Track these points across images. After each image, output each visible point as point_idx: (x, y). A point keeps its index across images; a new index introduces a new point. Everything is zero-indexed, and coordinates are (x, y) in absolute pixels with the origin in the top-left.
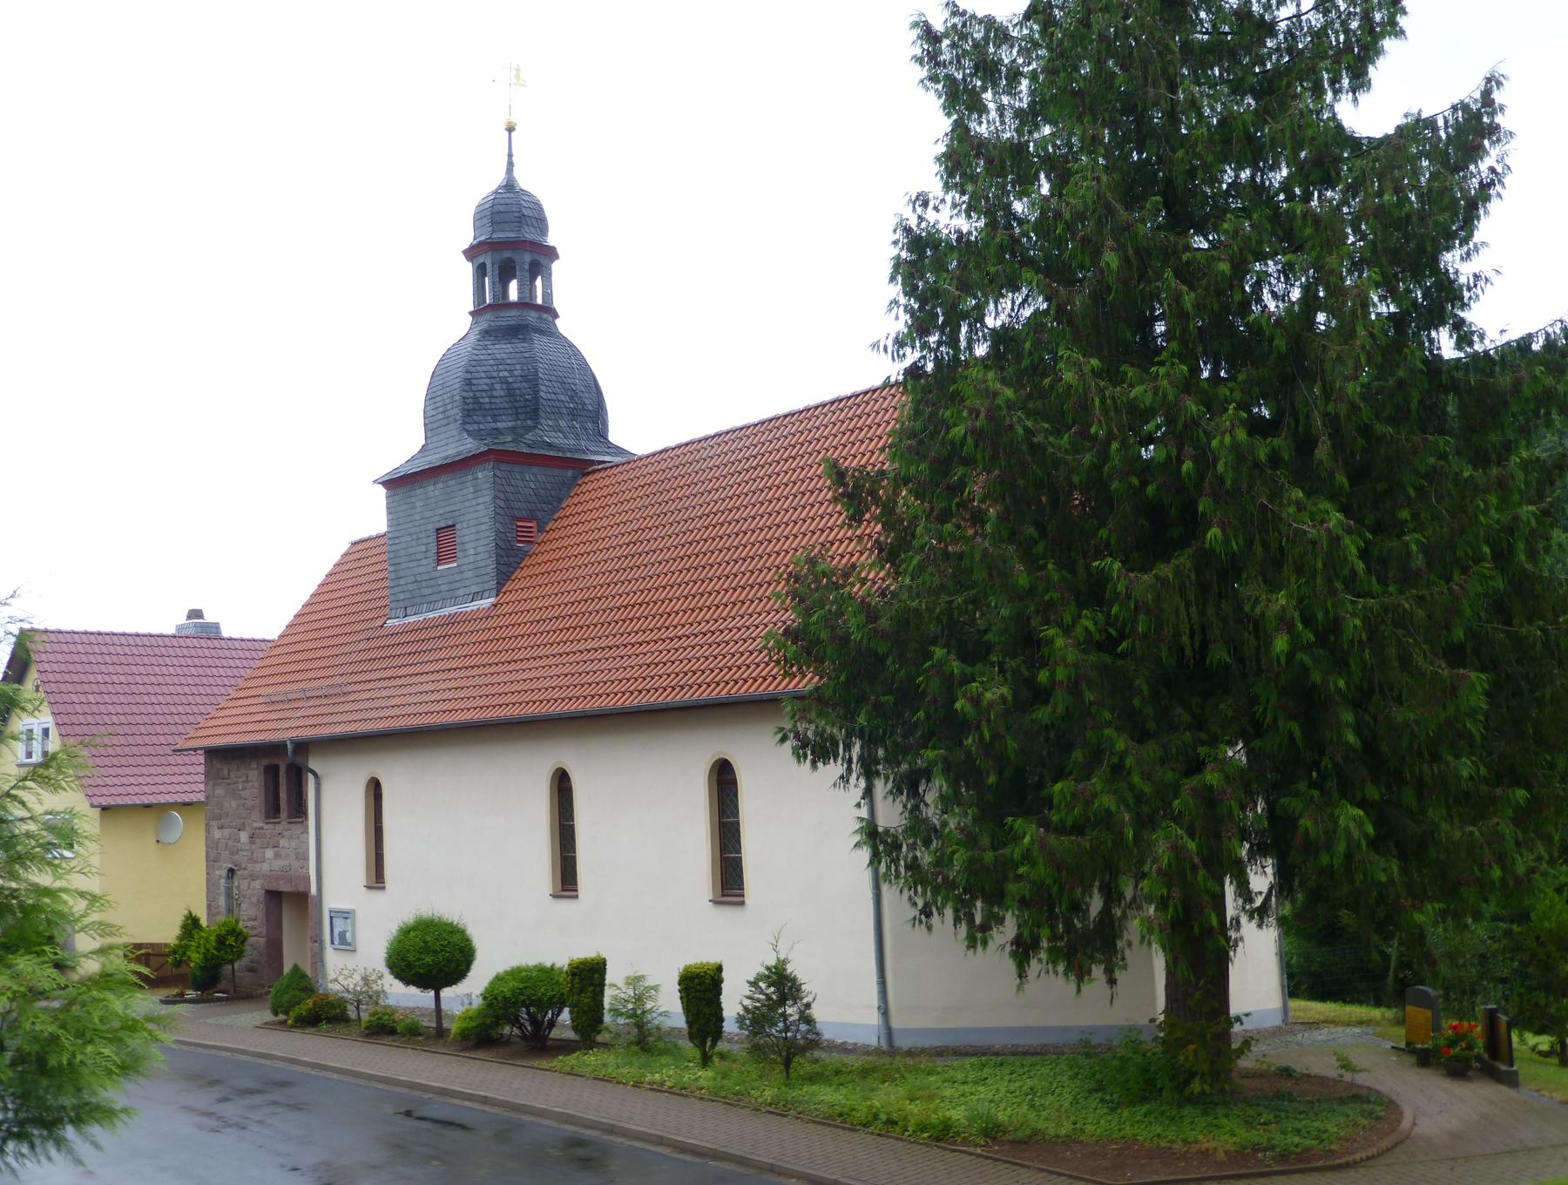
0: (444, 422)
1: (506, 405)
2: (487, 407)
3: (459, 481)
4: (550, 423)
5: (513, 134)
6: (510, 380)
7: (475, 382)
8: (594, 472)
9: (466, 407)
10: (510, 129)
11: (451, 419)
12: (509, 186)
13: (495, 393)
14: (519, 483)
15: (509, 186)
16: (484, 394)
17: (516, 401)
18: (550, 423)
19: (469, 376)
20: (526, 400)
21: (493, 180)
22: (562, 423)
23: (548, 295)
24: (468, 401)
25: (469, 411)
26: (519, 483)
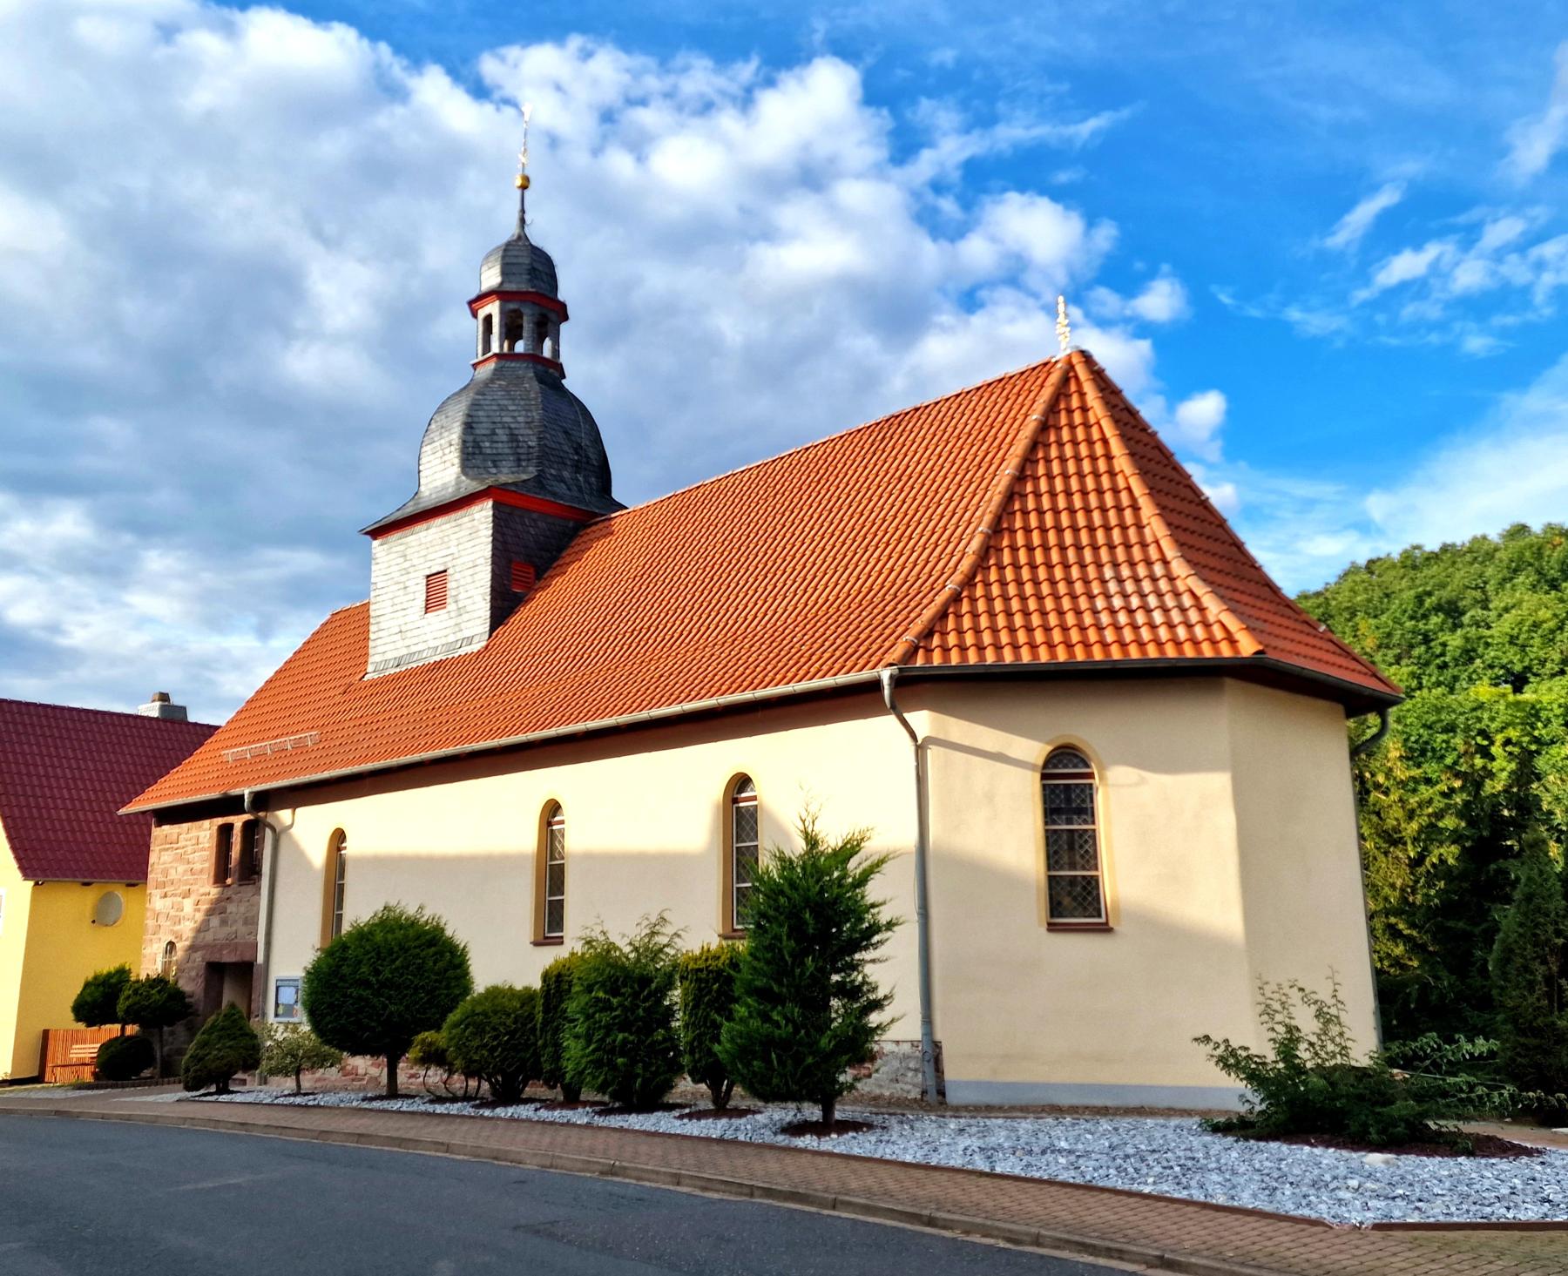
0: (442, 466)
1: (507, 451)
2: (488, 451)
3: (454, 524)
4: (553, 471)
5: (527, 192)
6: (513, 426)
7: (474, 425)
8: (596, 523)
9: (466, 451)
10: (524, 187)
11: (448, 464)
12: (522, 238)
13: (495, 438)
14: (519, 527)
15: (522, 238)
16: (485, 438)
17: (518, 447)
18: (553, 471)
19: (470, 420)
20: (529, 447)
21: (510, 230)
22: (566, 474)
23: (556, 352)
24: (468, 445)
25: (468, 454)
26: (519, 527)
